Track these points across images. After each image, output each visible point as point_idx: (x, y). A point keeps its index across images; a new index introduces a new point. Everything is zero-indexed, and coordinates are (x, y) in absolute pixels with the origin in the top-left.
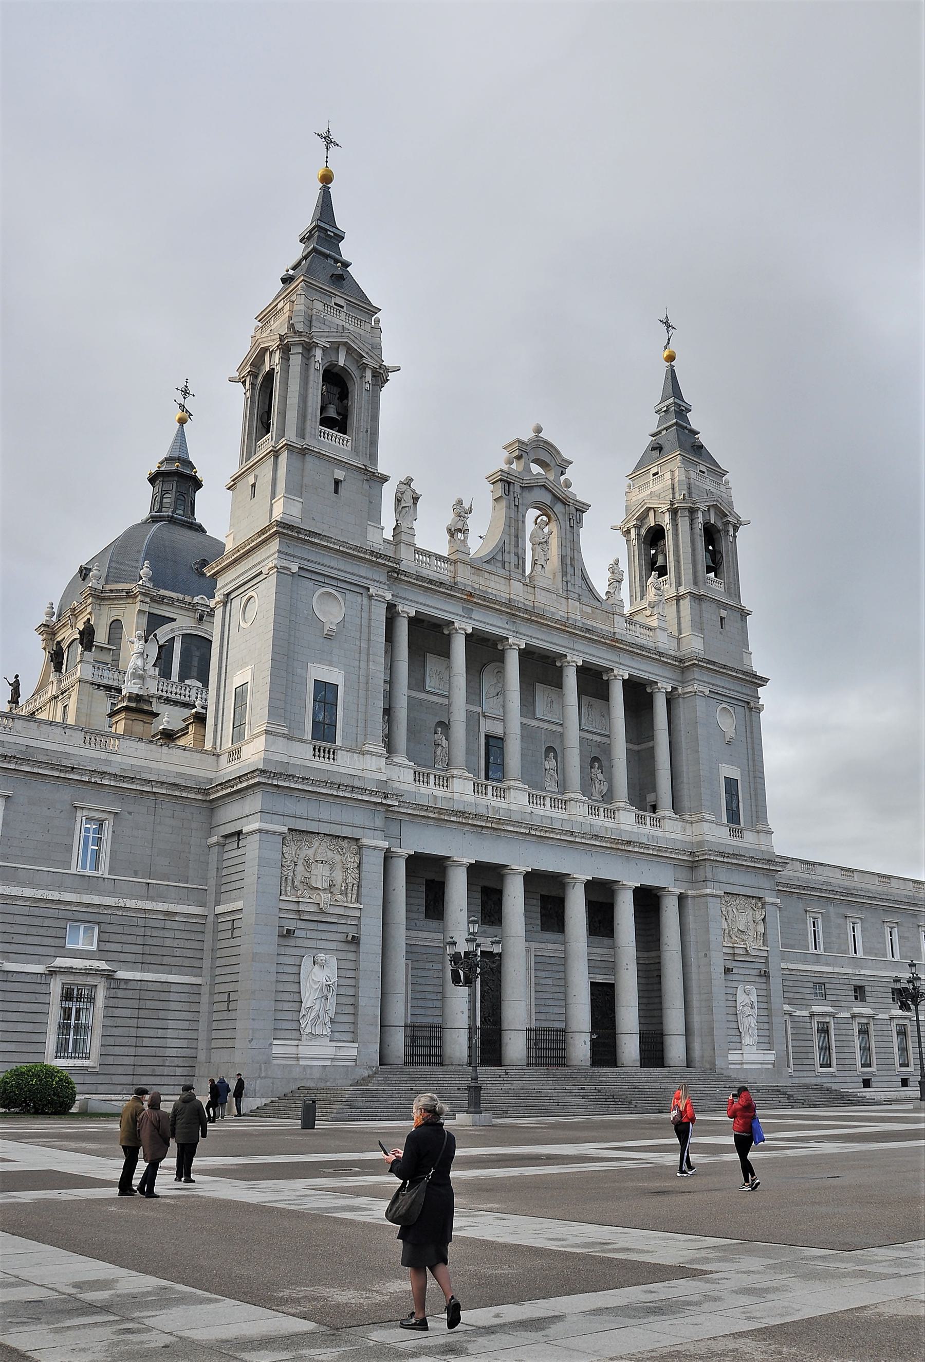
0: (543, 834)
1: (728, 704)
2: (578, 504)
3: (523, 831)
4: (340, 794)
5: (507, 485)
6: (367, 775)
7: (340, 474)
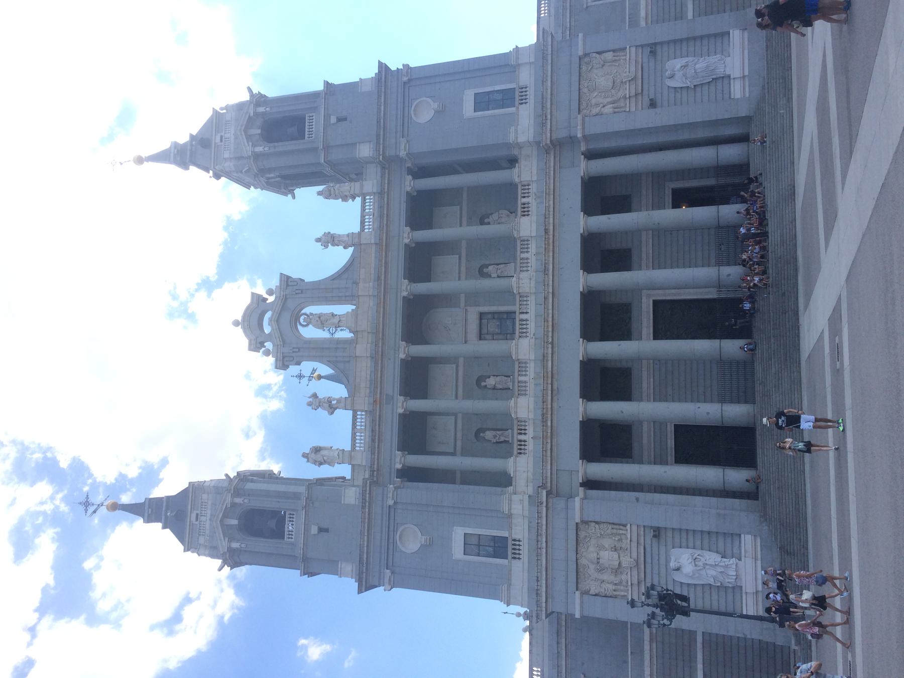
0: (550, 329)
1: (410, 108)
2: (282, 287)
3: (550, 351)
4: (544, 545)
5: (285, 359)
6: (526, 513)
7: (314, 530)
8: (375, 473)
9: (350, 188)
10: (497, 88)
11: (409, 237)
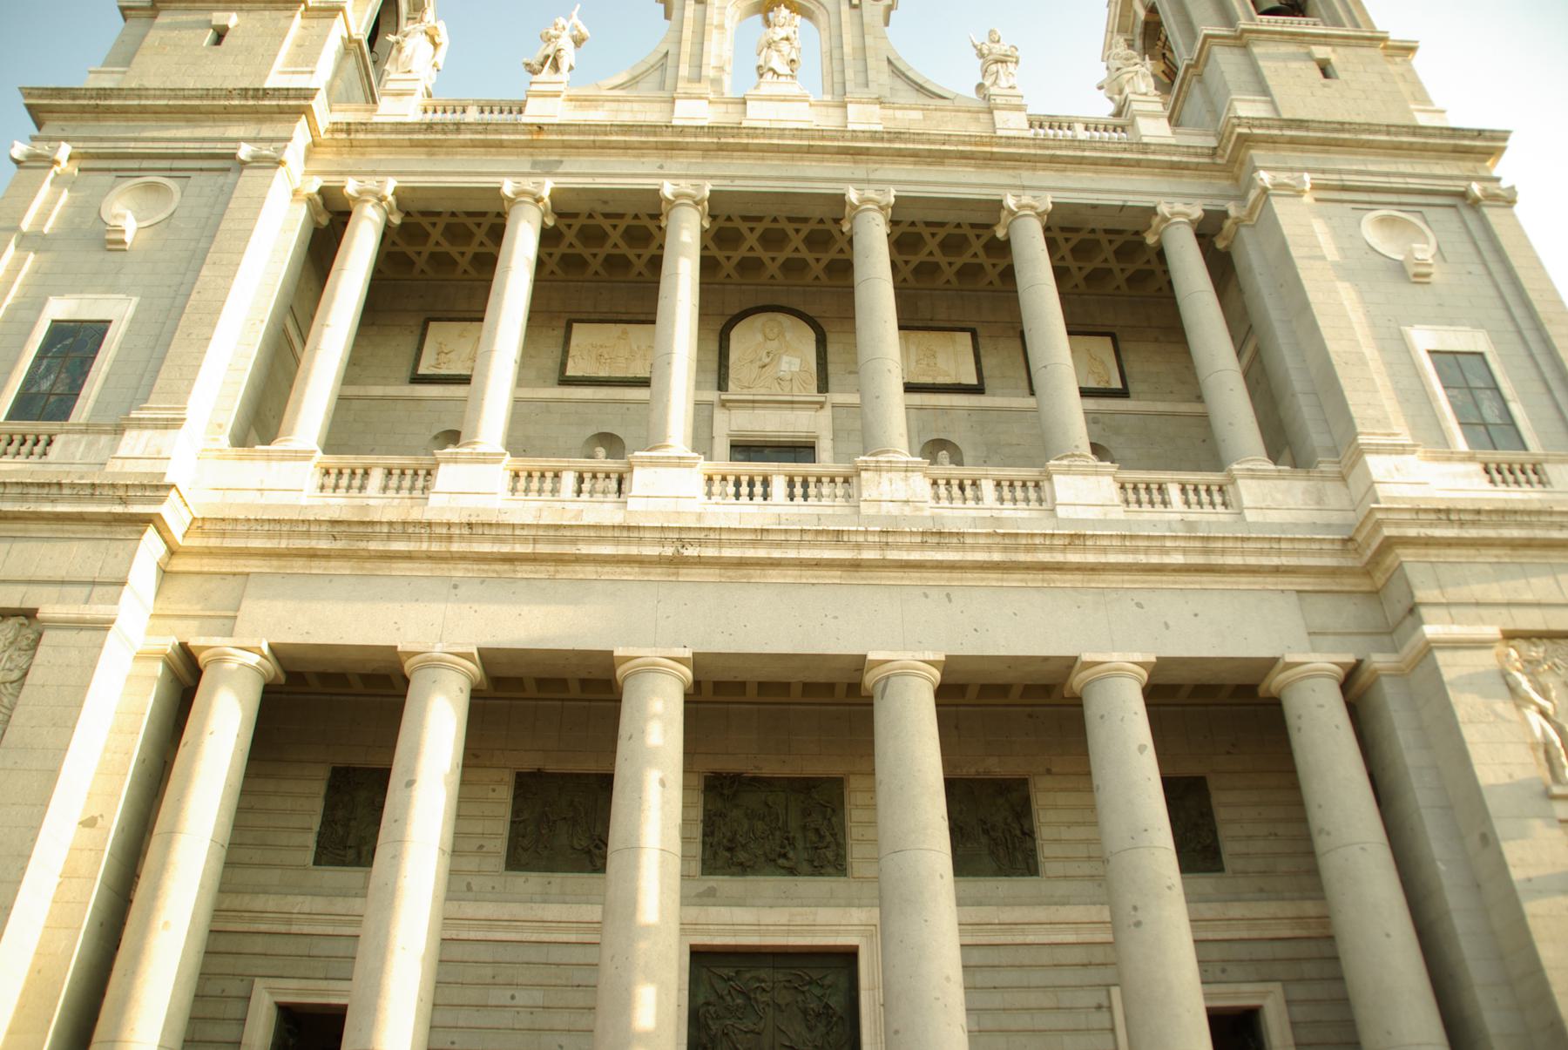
0: (728, 553)
8: (344, 136)
9: (1145, 94)
10: (1516, 409)
11: (1021, 207)
